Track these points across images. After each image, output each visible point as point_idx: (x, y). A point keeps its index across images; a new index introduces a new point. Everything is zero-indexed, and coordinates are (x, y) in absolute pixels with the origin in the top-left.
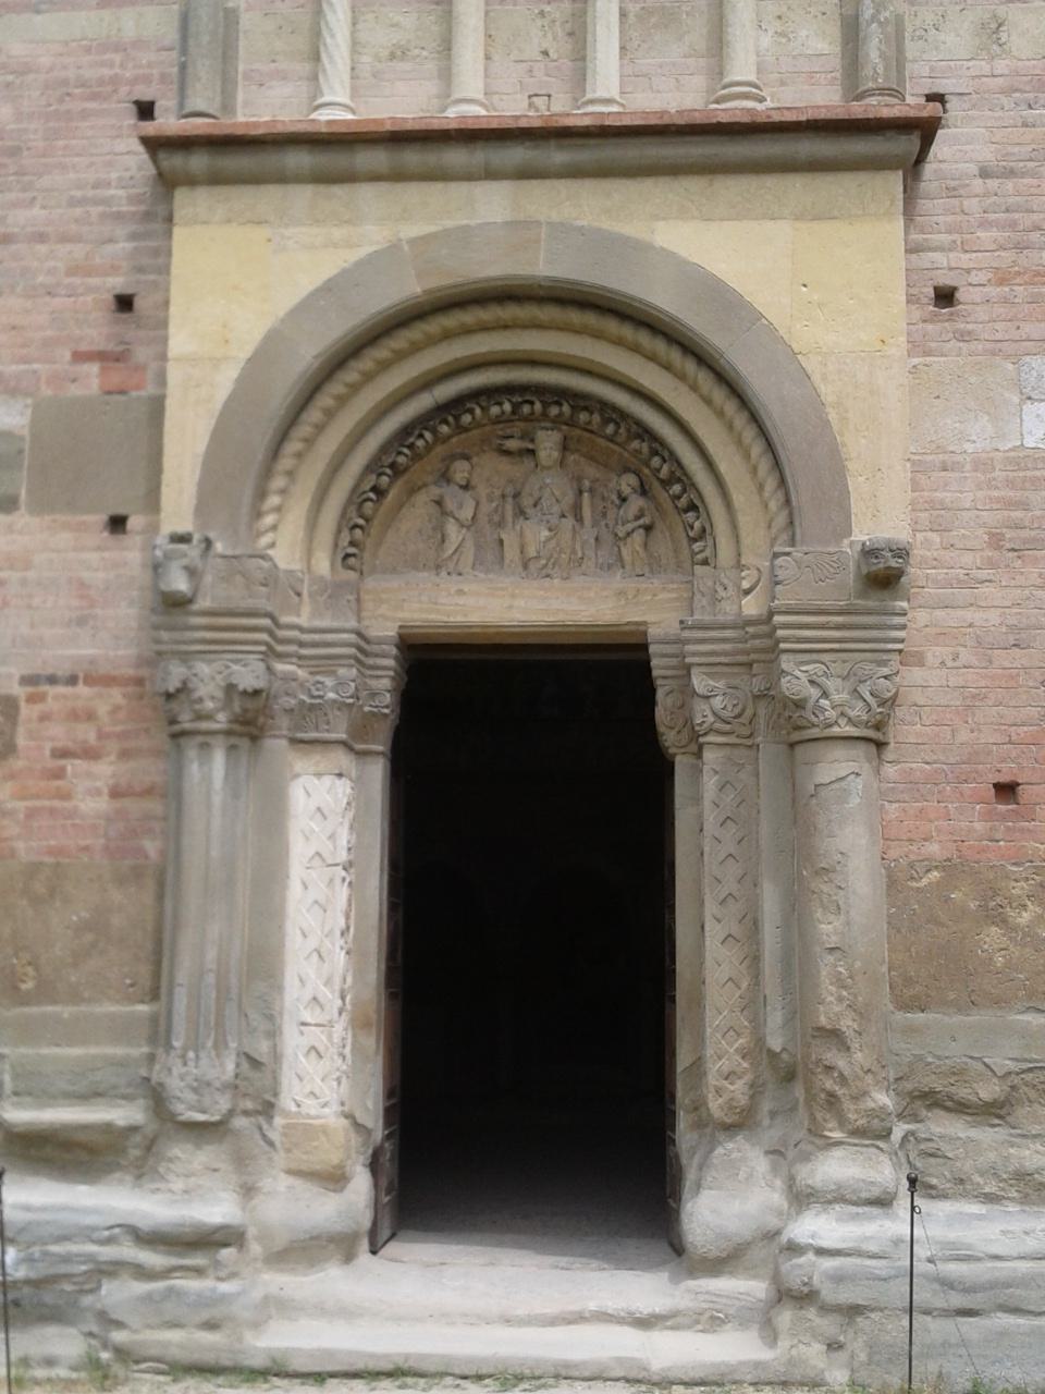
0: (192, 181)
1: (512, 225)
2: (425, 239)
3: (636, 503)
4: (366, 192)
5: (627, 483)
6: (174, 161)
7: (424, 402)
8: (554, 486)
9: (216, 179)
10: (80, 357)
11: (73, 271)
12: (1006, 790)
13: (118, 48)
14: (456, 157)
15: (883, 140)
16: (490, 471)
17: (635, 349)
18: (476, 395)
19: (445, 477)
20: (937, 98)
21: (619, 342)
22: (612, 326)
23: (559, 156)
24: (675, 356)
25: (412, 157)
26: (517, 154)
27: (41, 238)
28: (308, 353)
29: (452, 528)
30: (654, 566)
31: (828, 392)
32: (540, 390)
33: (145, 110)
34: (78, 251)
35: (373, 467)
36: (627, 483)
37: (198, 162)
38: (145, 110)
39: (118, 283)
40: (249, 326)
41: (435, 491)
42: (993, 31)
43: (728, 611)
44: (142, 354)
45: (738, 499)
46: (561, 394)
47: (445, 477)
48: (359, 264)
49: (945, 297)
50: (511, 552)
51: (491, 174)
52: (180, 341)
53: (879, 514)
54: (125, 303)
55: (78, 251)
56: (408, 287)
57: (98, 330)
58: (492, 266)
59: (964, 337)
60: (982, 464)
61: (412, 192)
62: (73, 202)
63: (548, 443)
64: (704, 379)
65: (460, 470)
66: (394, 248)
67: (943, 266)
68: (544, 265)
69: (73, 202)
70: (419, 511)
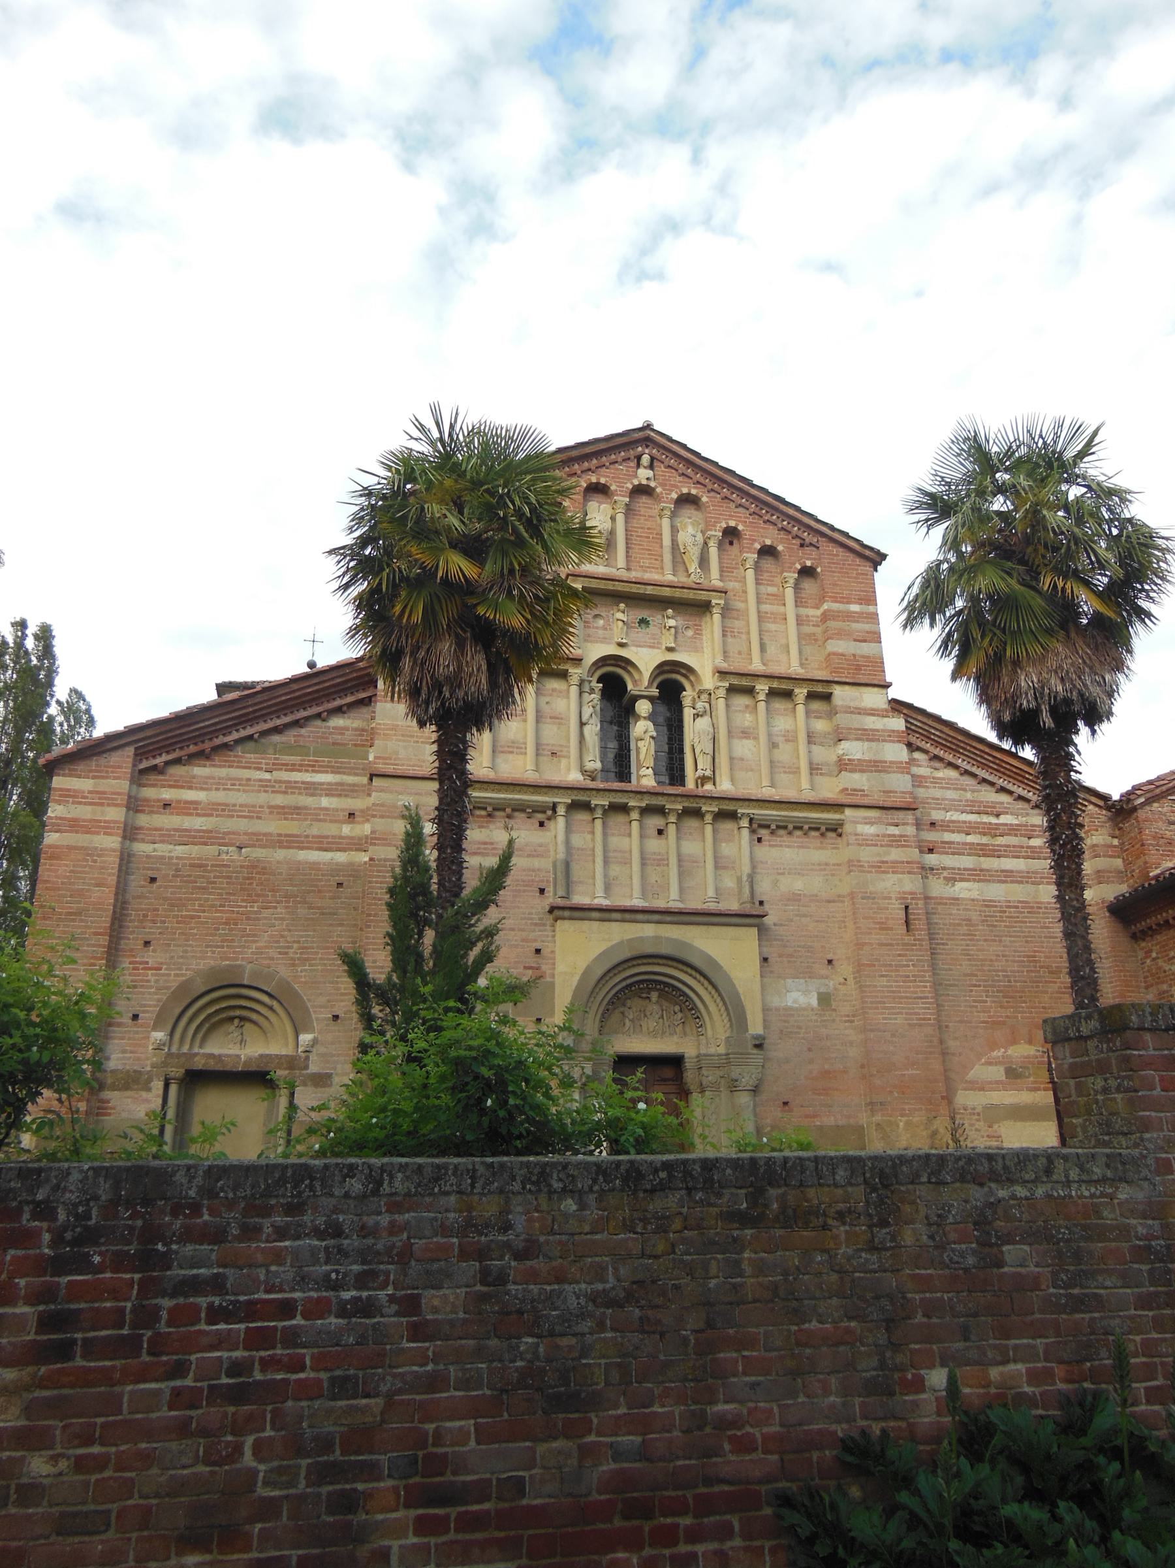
0: (564, 918)
1: (656, 937)
2: (632, 939)
3: (680, 1015)
4: (614, 924)
5: (677, 1008)
6: (557, 913)
7: (624, 984)
8: (653, 1008)
9: (571, 918)
10: (526, 968)
11: (523, 940)
12: (785, 1103)
13: (533, 871)
14: (640, 917)
15: (751, 917)
16: (636, 1003)
17: (686, 973)
18: (636, 982)
19: (624, 1005)
20: (761, 903)
21: (682, 970)
22: (680, 966)
23: (668, 918)
24: (698, 976)
25: (627, 916)
26: (656, 917)
27: (513, 930)
28: (599, 972)
29: (627, 1021)
30: (685, 1034)
31: (741, 991)
32: (655, 981)
33: (542, 891)
34: (524, 934)
35: (608, 1004)
36: (677, 1008)
37: (567, 913)
38: (542, 891)
39: (538, 945)
40: (582, 966)
41: (622, 1009)
42: (775, 883)
43: (712, 1051)
44: (544, 967)
45: (715, 1018)
46: (660, 982)
47: (624, 1005)
48: (612, 947)
49: (765, 960)
50: (645, 1029)
51: (648, 922)
52: (560, 968)
53: (755, 1027)
54: (538, 951)
55: (524, 934)
56: (628, 954)
57: (532, 960)
58: (650, 950)
59: (772, 972)
60: (777, 1009)
61: (627, 925)
62: (522, 919)
63: (654, 996)
64: (706, 983)
65: (629, 1003)
66: (622, 942)
67: (767, 951)
68: (664, 950)
69: (522, 919)
70: (616, 1016)
